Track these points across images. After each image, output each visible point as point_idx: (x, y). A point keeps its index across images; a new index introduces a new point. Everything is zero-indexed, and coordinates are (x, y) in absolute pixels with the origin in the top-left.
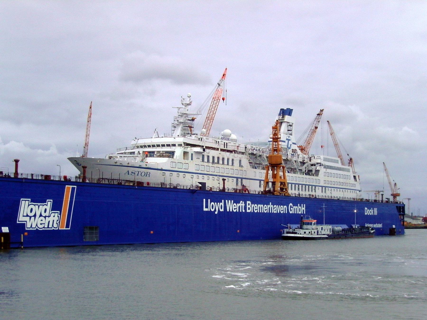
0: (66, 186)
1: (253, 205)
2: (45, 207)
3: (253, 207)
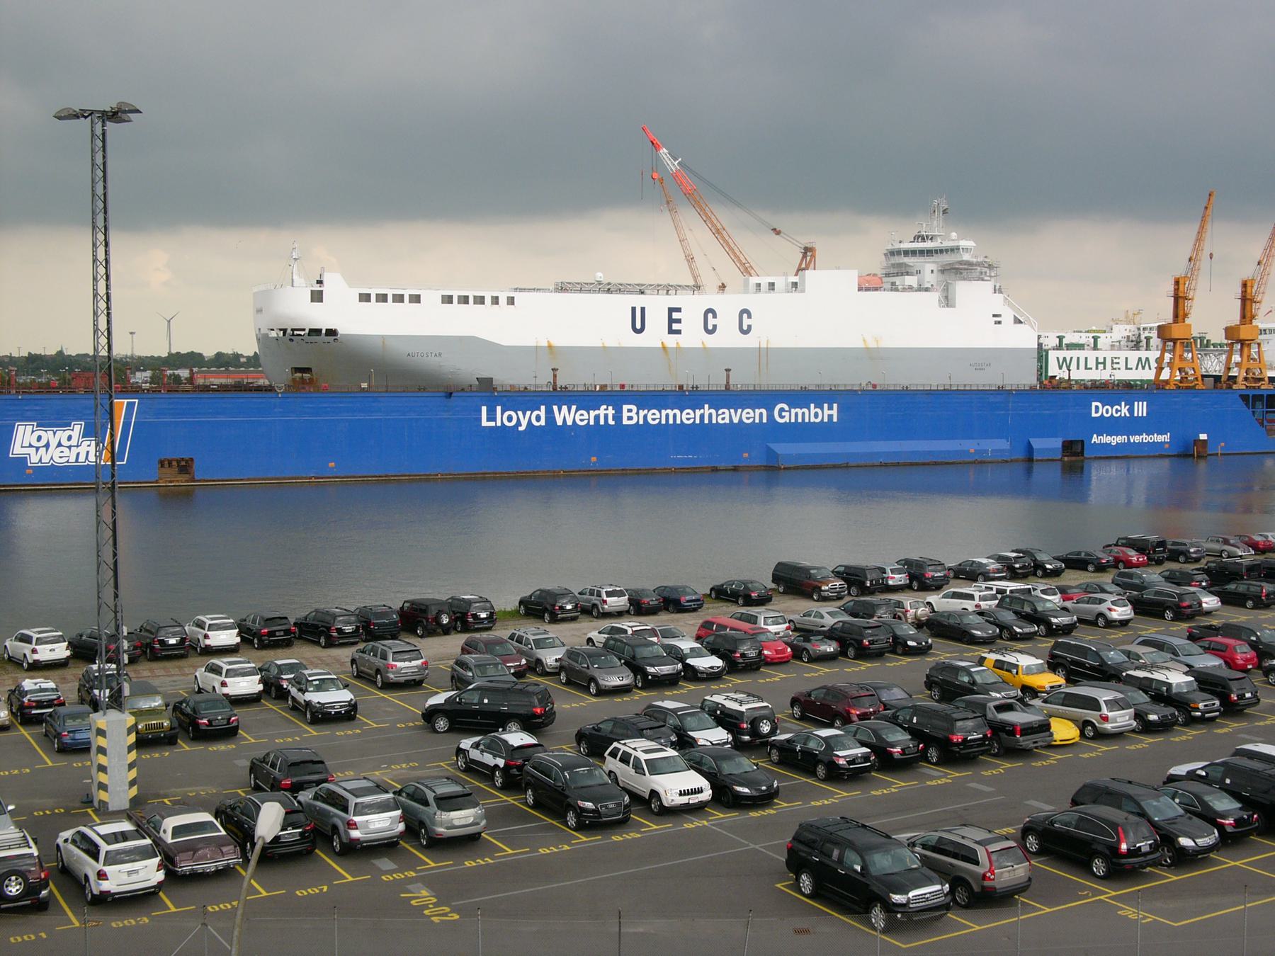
1: (642, 413)
2: (68, 433)
3: (645, 417)
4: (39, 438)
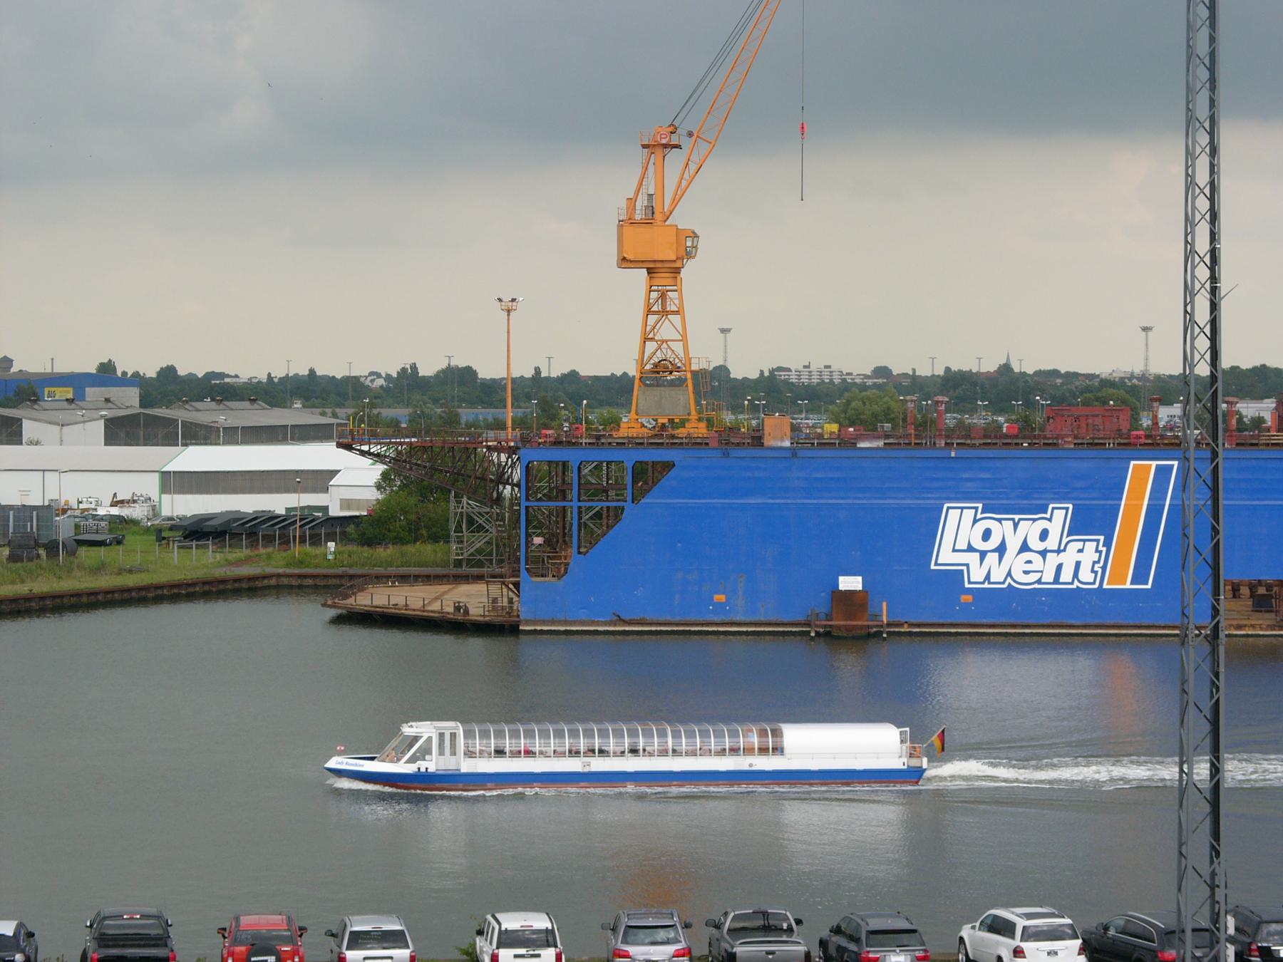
0: (1132, 463)
4: (987, 535)
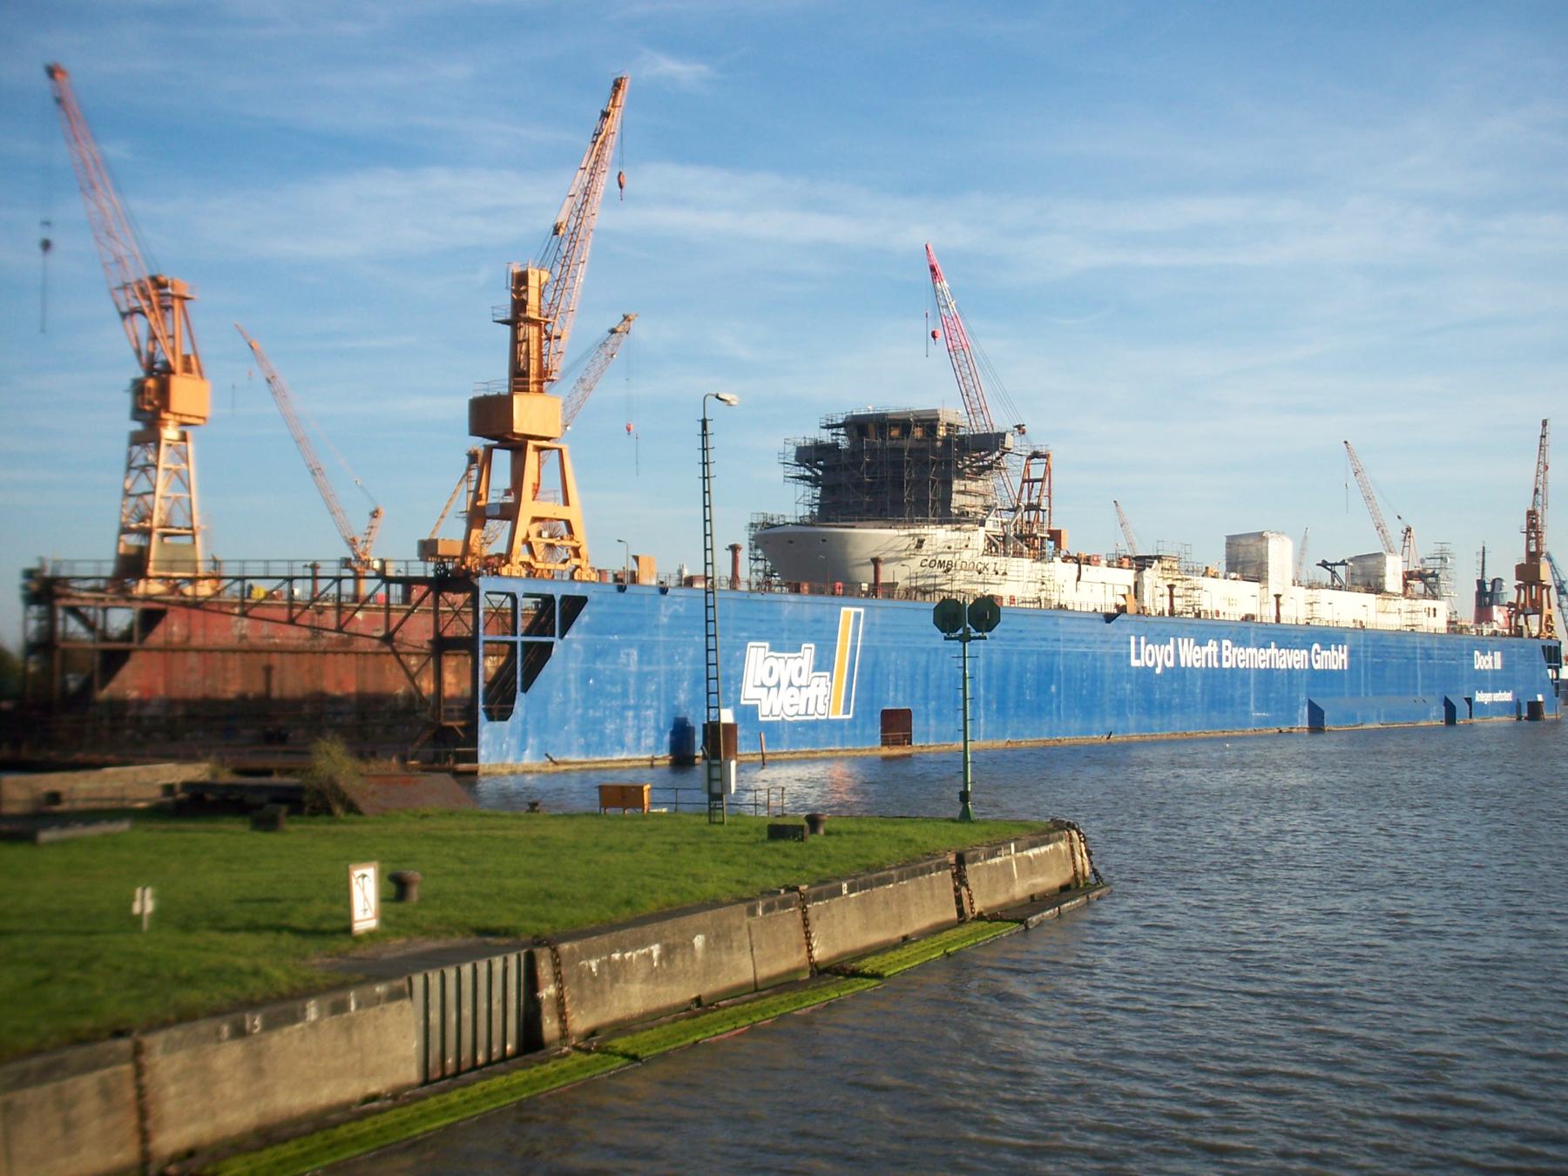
1: (1235, 650)
2: (799, 662)
